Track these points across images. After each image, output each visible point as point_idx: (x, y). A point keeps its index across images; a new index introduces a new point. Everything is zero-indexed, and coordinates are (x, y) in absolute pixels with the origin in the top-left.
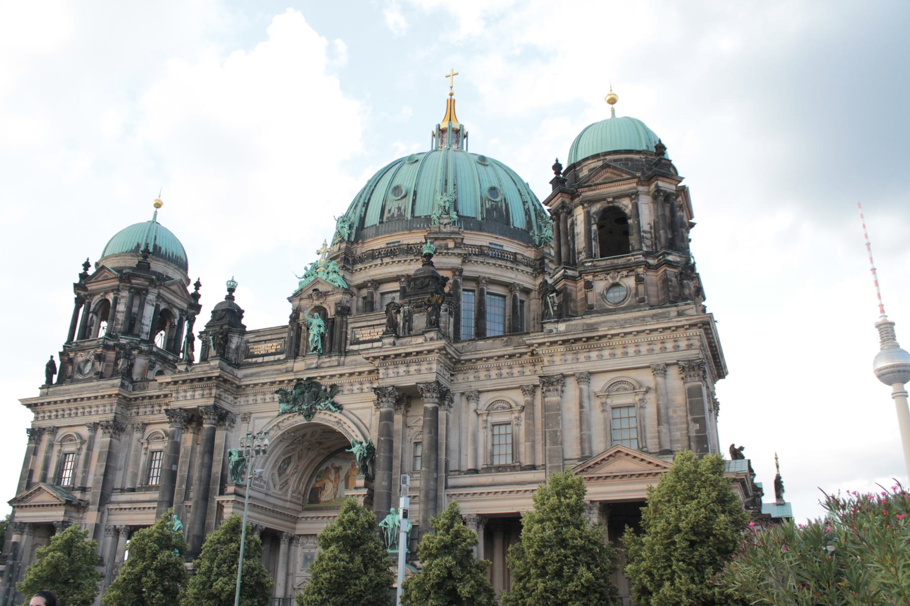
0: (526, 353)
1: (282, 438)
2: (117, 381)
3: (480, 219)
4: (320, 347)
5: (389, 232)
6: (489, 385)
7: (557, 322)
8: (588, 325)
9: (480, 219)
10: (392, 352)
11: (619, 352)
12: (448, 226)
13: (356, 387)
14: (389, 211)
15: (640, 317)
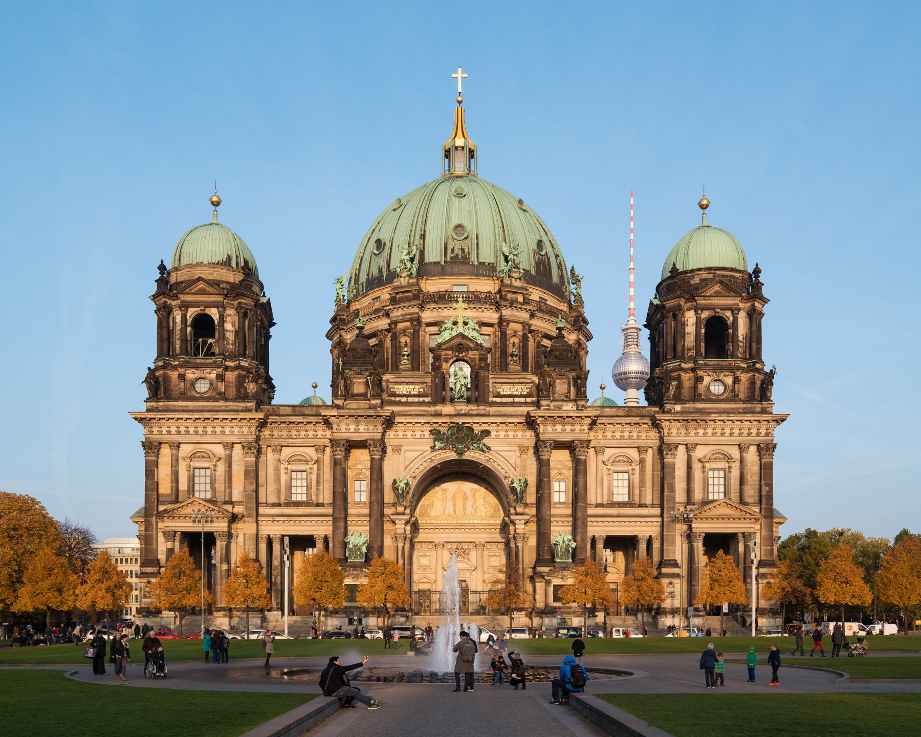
0: (647, 424)
1: (432, 468)
2: (251, 405)
3: (533, 272)
4: (465, 396)
5: (456, 275)
6: (614, 443)
7: (675, 404)
8: (697, 409)
9: (533, 272)
10: (555, 414)
11: (719, 431)
12: (518, 280)
13: (502, 434)
14: (453, 250)
15: (735, 408)
